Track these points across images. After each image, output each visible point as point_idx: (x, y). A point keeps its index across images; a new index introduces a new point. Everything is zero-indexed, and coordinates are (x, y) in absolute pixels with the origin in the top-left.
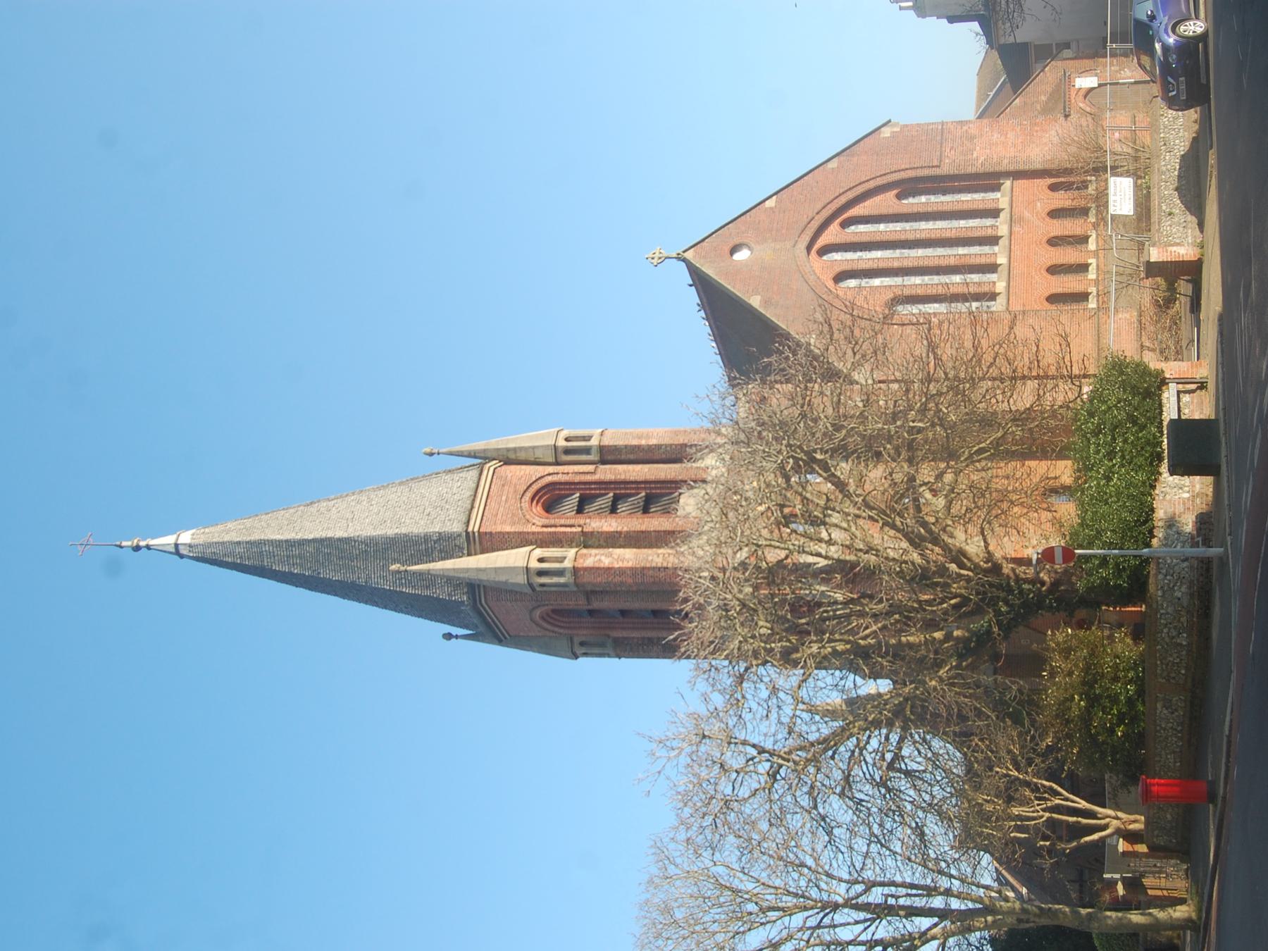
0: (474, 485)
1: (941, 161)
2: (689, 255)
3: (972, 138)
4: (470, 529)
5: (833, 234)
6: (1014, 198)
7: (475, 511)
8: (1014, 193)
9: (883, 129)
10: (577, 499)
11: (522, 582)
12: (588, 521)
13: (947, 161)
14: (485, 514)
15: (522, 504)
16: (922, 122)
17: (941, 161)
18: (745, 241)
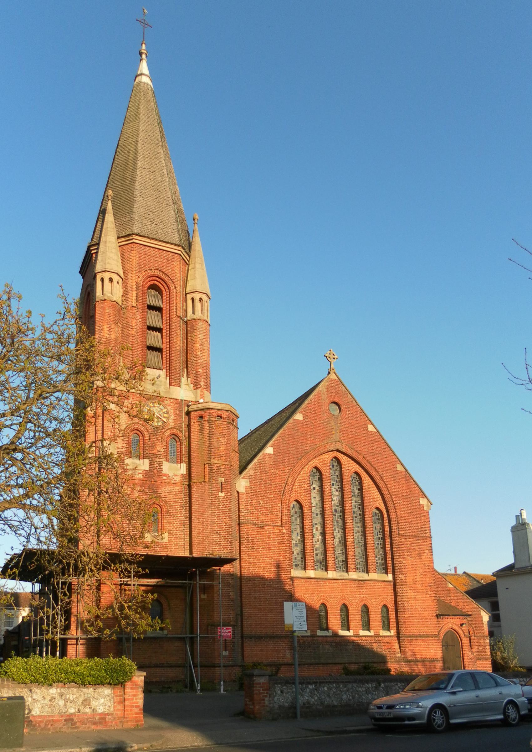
0: (167, 241)
1: (403, 536)
2: (333, 376)
3: (420, 555)
4: (134, 237)
5: (349, 466)
6: (376, 582)
7: (149, 241)
8: (380, 583)
9: (425, 500)
10: (158, 306)
11: (96, 269)
12: (141, 311)
13: (403, 540)
14: (146, 247)
15: (154, 271)
16: (431, 525)
17: (403, 536)
18: (343, 411)
